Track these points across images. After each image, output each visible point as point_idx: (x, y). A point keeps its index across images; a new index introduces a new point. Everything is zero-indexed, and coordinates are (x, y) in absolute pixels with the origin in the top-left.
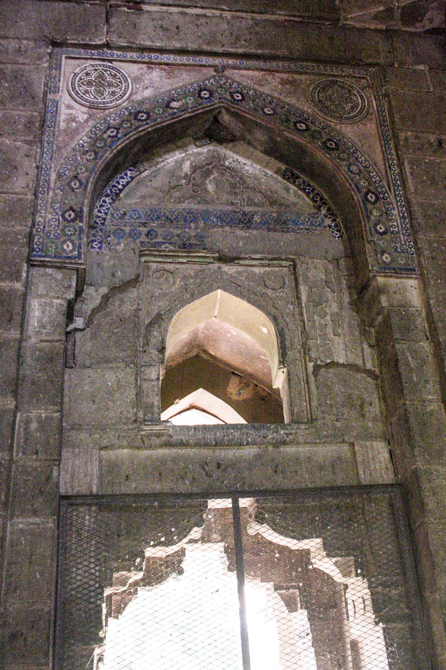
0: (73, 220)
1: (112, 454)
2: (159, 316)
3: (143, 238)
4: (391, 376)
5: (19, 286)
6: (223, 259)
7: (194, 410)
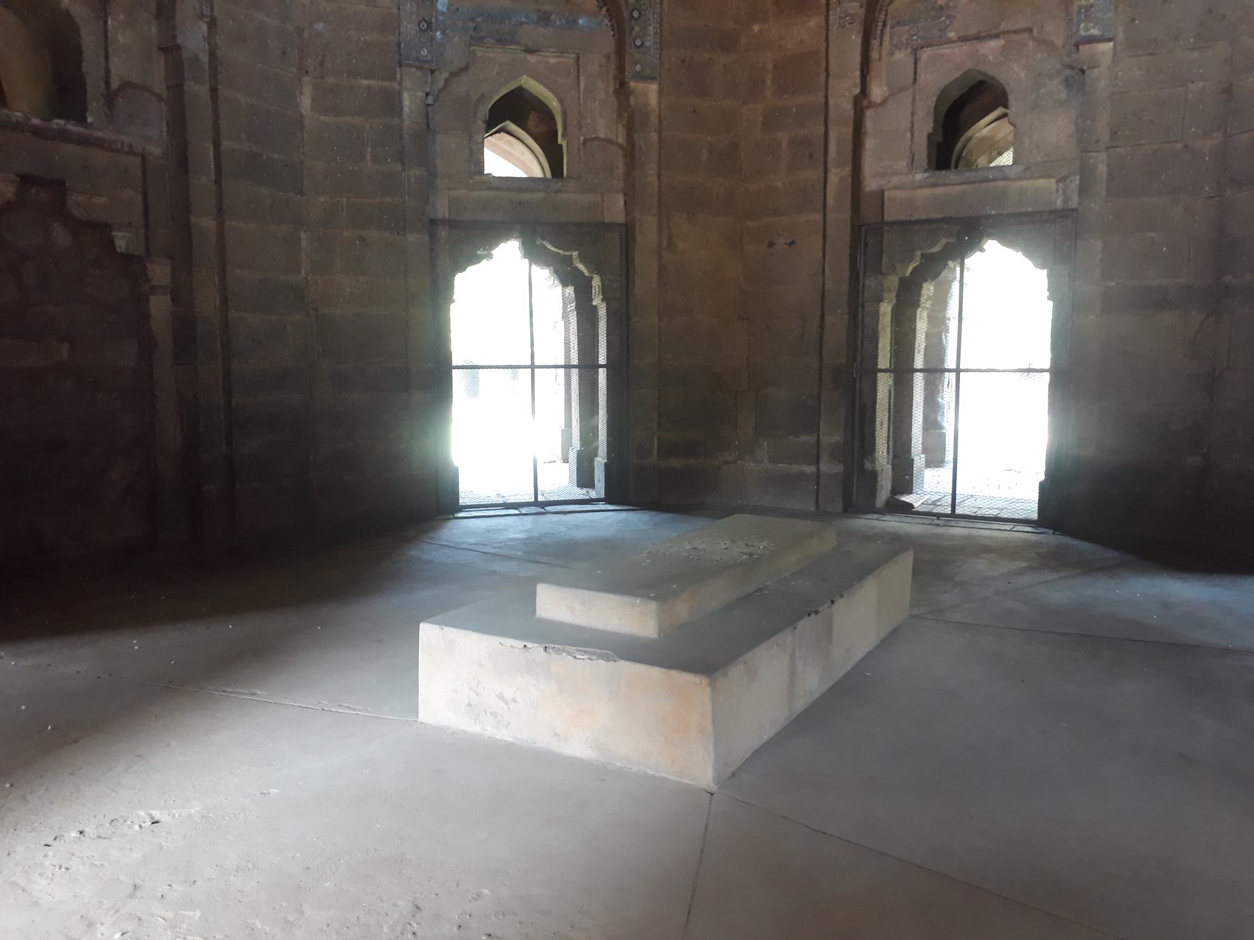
0: (426, 30)
1: (455, 193)
2: (483, 95)
3: (471, 32)
4: (630, 152)
5: (395, 85)
6: (530, 51)
7: (503, 134)
